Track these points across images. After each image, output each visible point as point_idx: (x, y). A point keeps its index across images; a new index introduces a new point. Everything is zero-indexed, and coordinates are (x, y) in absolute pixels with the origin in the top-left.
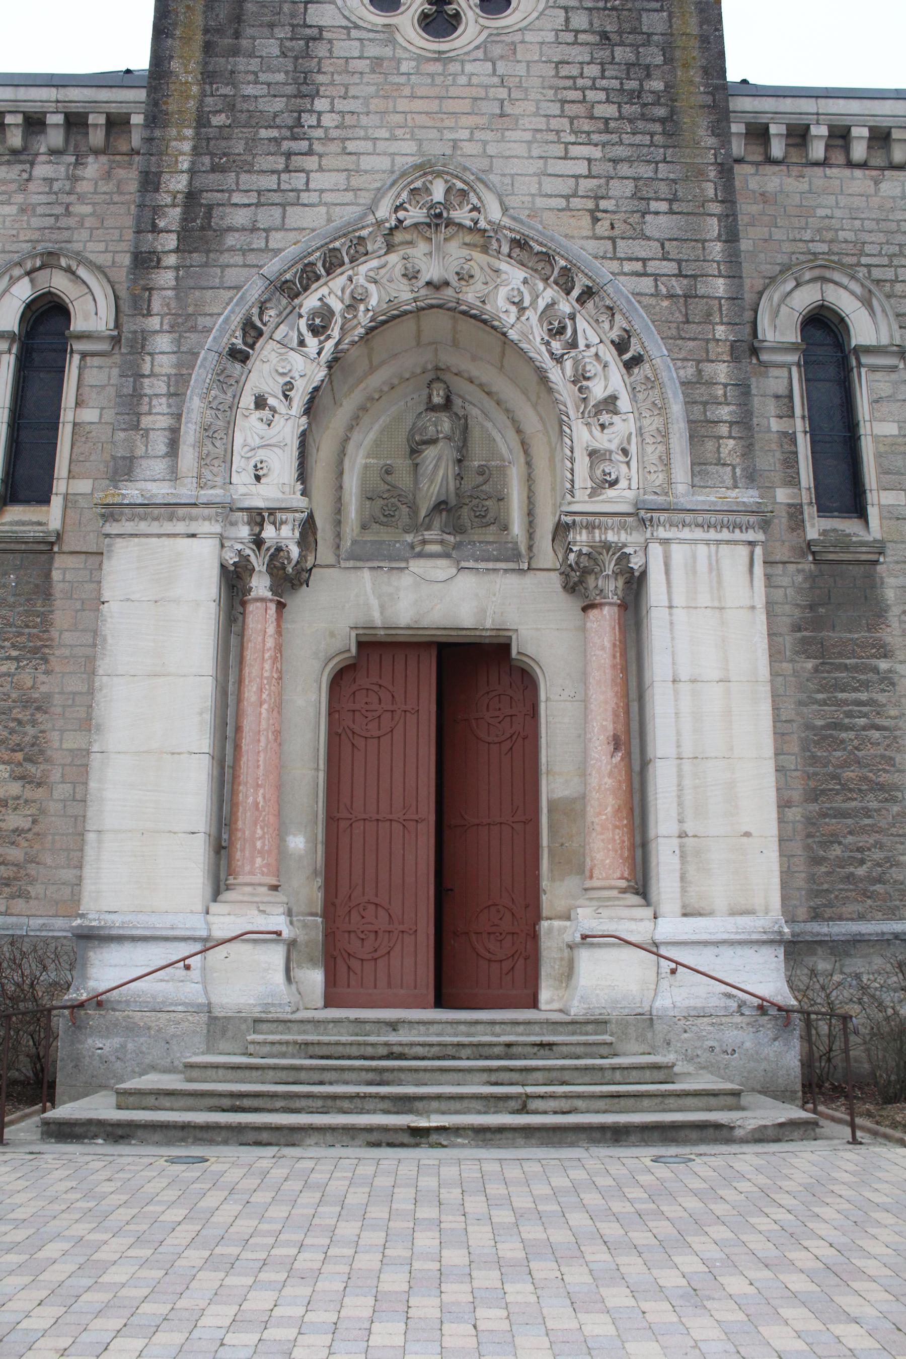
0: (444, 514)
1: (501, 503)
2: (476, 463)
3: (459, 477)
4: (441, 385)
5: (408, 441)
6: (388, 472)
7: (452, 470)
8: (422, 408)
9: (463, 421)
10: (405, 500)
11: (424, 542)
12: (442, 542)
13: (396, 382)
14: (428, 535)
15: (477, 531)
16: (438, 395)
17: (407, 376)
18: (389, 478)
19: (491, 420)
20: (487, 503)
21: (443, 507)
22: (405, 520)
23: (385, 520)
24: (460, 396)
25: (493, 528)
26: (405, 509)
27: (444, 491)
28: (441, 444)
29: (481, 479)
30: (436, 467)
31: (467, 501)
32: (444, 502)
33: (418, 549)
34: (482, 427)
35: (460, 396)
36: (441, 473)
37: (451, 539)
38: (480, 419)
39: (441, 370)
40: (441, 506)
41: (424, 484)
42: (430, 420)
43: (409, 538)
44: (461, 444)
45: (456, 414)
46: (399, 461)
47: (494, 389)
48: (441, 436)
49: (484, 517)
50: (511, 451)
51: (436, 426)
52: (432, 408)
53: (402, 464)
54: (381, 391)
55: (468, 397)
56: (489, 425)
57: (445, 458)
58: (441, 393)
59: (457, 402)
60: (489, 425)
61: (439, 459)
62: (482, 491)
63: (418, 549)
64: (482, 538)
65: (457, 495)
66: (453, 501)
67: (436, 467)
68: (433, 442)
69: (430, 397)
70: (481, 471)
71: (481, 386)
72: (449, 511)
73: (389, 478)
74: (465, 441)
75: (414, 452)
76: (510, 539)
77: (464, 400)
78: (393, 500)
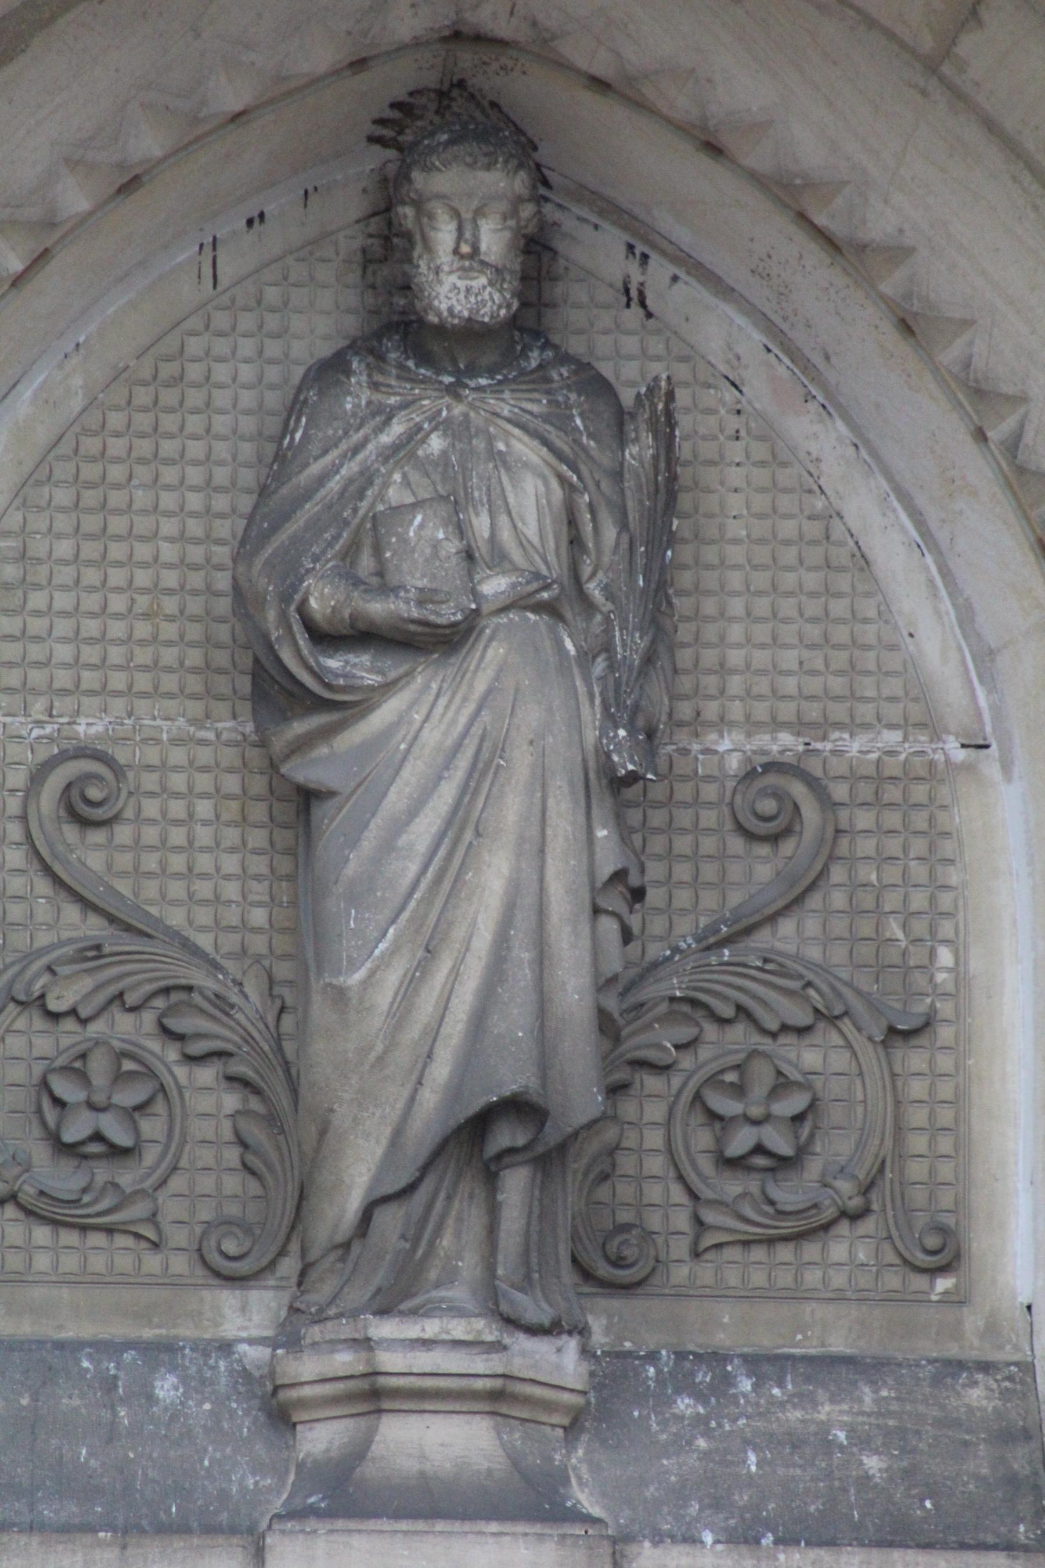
0: (516, 1185)
1: (914, 1058)
2: (730, 749)
3: (623, 892)
4: (499, 182)
5: (242, 597)
6: (81, 813)
7: (573, 847)
8: (323, 316)
9: (639, 451)
10: (218, 1033)
11: (373, 1396)
12: (498, 1399)
13: (147, 143)
14: (402, 1345)
15: (733, 1268)
16: (471, 258)
17: (231, 96)
18: (89, 855)
19: (833, 405)
20: (811, 1058)
21: (506, 1135)
22: (204, 1180)
23: (64, 1179)
24: (612, 211)
25: (848, 1249)
26: (208, 1100)
27: (514, 1021)
28: (491, 656)
29: (762, 870)
30: (463, 829)
31: (667, 1038)
32: (516, 1107)
33: (321, 1438)
34: (777, 454)
35: (612, 211)
36: (495, 874)
37: (560, 1363)
38: (758, 391)
39: (479, 38)
40: (484, 1137)
41: (372, 968)
42: (403, 450)
43: (245, 1318)
44: (630, 645)
45: (596, 386)
46: (166, 722)
47: (880, 223)
48: (495, 586)
49: (783, 1164)
50: (985, 659)
51: (455, 506)
52: (400, 332)
53: (181, 745)
54: (50, 224)
55: (665, 222)
56: (819, 439)
57: (521, 761)
58: (493, 239)
59: (597, 252)
60: (819, 439)
61: (478, 772)
62: (773, 965)
63: (321, 1438)
64: (767, 1330)
65: (606, 1024)
66: (580, 1097)
67: (463, 829)
68: (436, 641)
69: (388, 247)
70: (772, 807)
71: (791, 195)
72: (548, 1161)
73: (89, 855)
74: (657, 605)
75: (276, 693)
76: (974, 1348)
77: (643, 242)
78: (125, 1023)
